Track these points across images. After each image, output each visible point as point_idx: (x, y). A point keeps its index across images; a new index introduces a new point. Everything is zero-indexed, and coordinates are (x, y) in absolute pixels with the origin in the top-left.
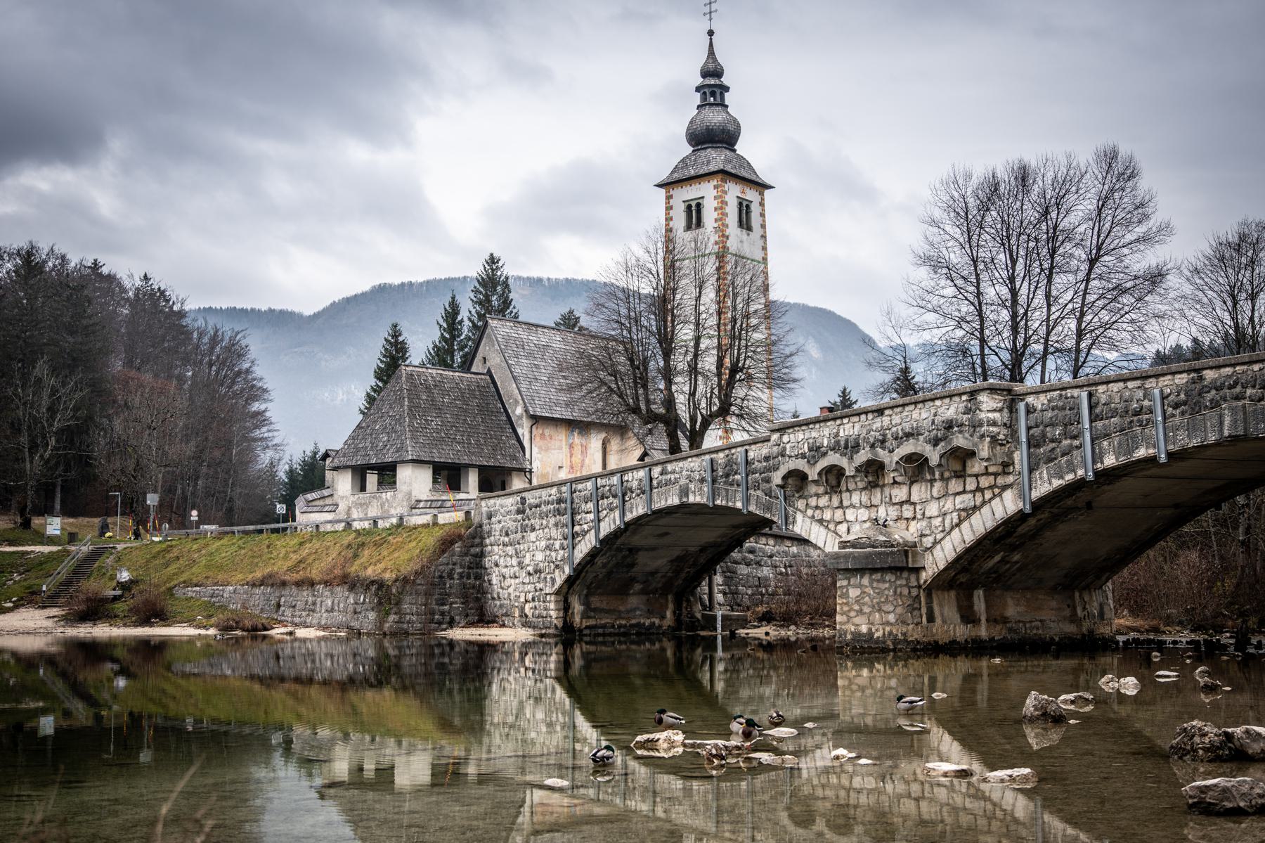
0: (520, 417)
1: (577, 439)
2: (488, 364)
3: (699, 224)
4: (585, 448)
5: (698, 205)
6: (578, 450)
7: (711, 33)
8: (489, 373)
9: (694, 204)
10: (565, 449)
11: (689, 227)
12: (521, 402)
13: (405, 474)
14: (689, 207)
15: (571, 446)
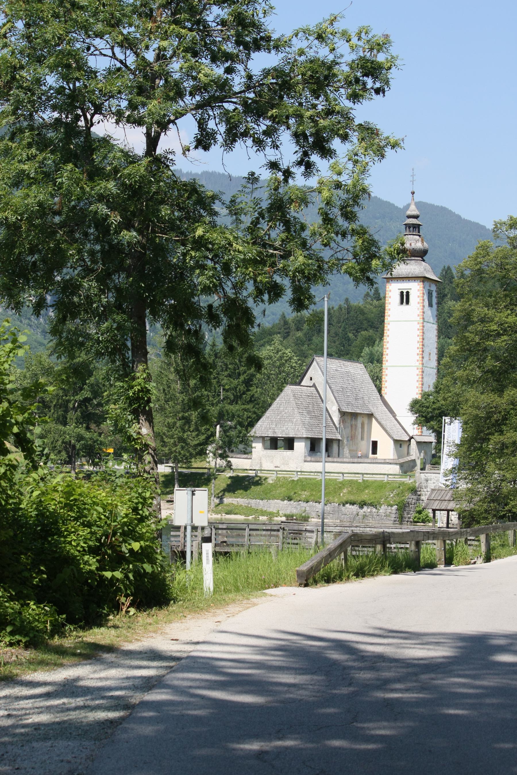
0: (335, 412)
1: (353, 423)
2: (313, 381)
3: (408, 302)
4: (356, 426)
5: (408, 293)
6: (354, 426)
7: (413, 193)
8: (314, 386)
9: (405, 291)
10: (350, 426)
11: (402, 303)
12: (336, 404)
13: (296, 445)
14: (402, 293)
15: (352, 426)
